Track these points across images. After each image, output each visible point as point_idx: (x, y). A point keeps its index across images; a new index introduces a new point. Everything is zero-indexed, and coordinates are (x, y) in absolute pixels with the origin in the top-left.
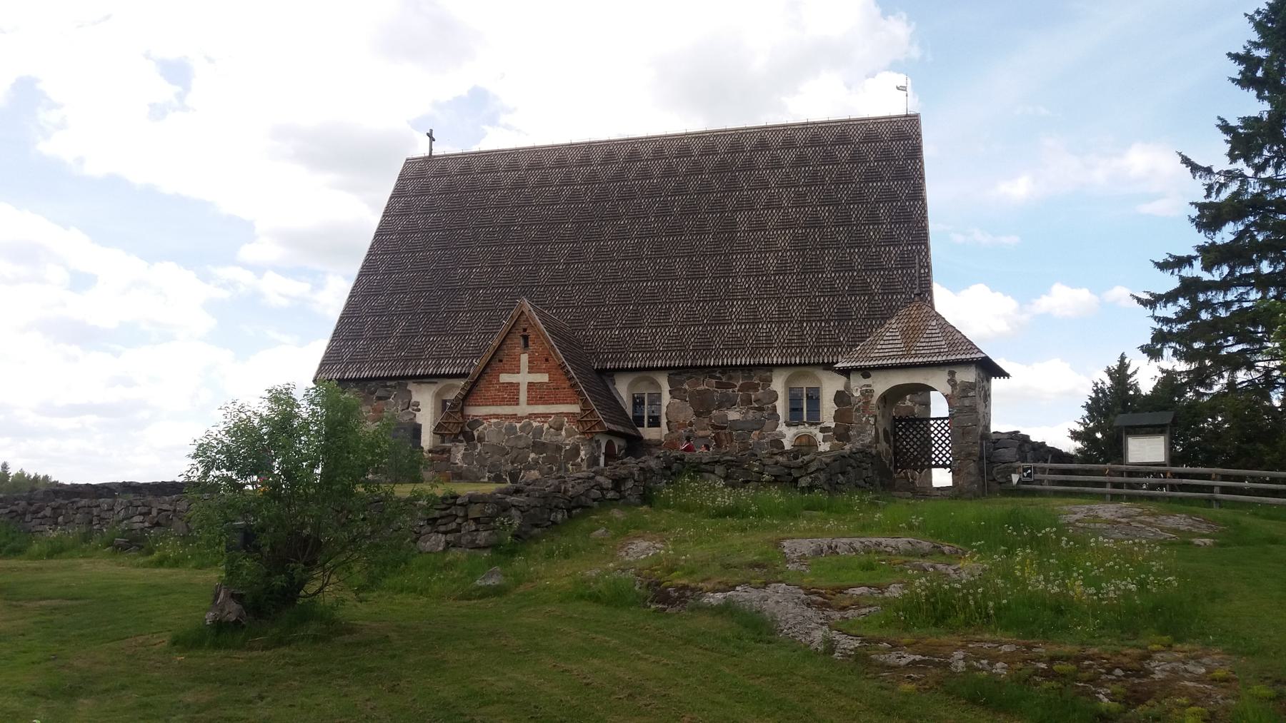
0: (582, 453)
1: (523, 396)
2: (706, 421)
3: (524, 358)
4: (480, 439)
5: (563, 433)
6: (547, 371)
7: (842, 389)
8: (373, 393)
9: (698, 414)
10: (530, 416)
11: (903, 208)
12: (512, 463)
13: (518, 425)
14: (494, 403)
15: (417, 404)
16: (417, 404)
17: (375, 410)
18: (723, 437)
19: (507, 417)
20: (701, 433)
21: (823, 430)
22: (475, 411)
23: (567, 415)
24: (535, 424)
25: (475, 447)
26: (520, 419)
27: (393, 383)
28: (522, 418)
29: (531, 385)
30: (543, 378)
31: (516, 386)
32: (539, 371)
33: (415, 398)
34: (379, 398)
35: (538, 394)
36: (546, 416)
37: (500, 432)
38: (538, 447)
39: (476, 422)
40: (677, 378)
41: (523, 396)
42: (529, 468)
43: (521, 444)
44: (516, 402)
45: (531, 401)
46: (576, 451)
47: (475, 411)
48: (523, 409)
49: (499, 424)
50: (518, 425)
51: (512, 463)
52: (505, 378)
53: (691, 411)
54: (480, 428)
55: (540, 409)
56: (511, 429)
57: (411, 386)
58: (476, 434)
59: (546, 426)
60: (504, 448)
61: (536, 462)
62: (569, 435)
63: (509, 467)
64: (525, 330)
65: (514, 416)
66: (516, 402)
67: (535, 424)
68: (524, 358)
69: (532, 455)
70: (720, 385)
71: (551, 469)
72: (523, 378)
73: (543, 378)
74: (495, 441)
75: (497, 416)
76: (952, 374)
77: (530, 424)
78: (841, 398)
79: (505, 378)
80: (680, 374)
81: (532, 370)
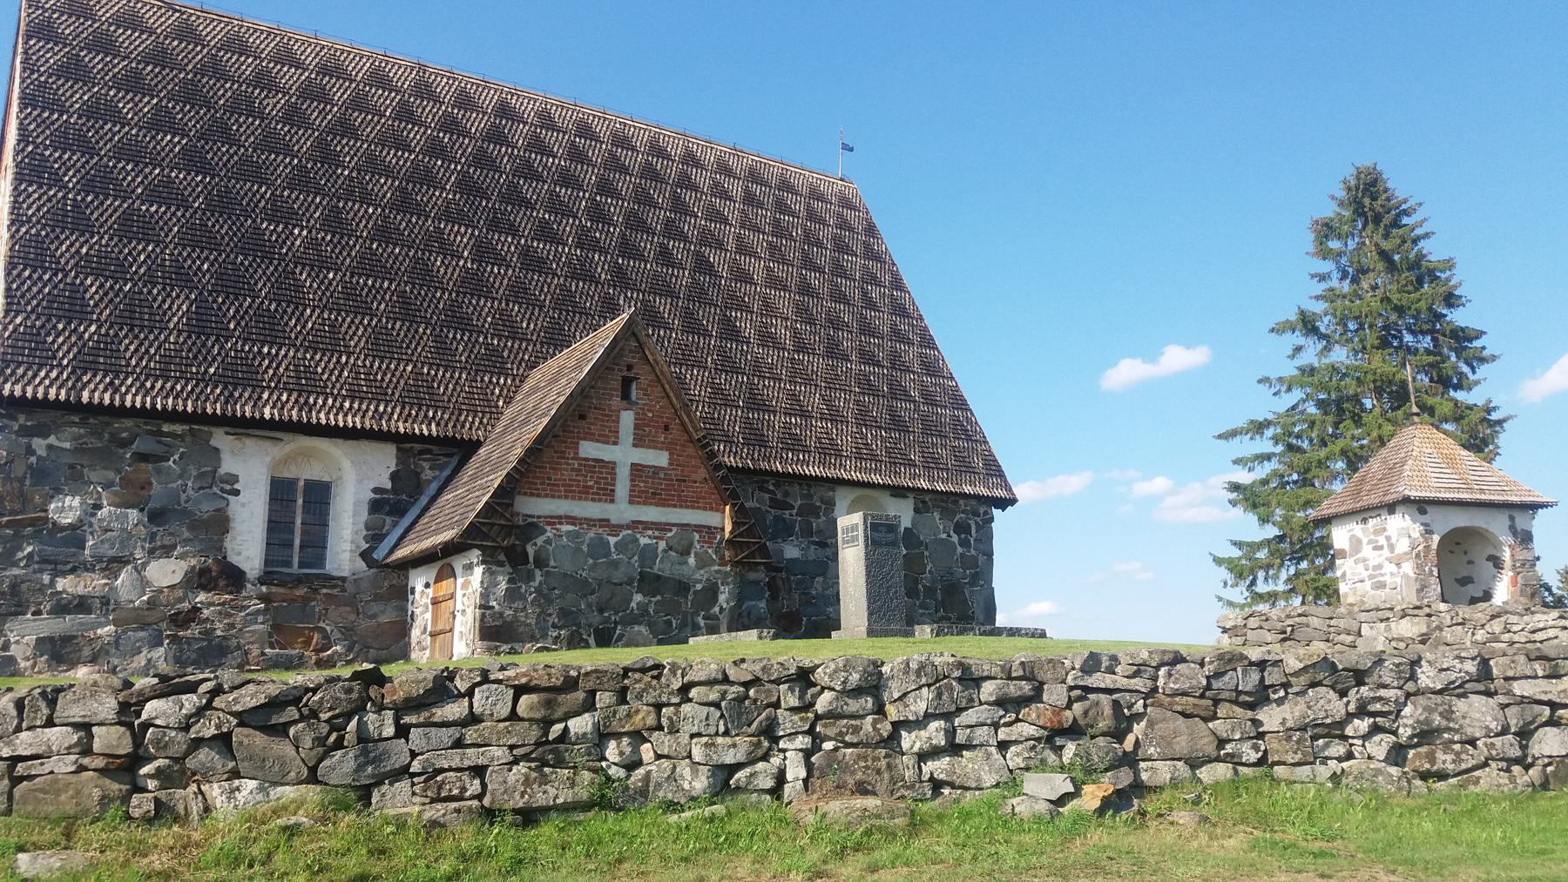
0: (722, 598)
1: (622, 487)
3: (627, 419)
4: (540, 562)
5: (692, 560)
6: (669, 447)
10: (635, 525)
12: (601, 611)
13: (612, 540)
14: (569, 494)
15: (233, 479)
16: (233, 479)
17: (126, 482)
18: (780, 583)
19: (590, 522)
22: (535, 506)
23: (699, 528)
24: (644, 541)
25: (530, 577)
26: (615, 529)
27: (179, 428)
28: (621, 527)
29: (637, 469)
30: (660, 459)
32: (654, 445)
33: (228, 465)
34: (142, 457)
35: (647, 486)
37: (578, 550)
38: (650, 582)
39: (531, 529)
41: (622, 487)
43: (618, 576)
44: (608, 495)
46: (712, 592)
47: (535, 506)
48: (622, 510)
49: (577, 535)
51: (601, 611)
52: (589, 449)
54: (540, 541)
55: (652, 513)
56: (599, 547)
57: (220, 439)
58: (531, 550)
59: (662, 545)
61: (643, 609)
62: (703, 563)
63: (596, 619)
64: (630, 368)
65: (604, 523)
66: (608, 495)
68: (627, 419)
69: (638, 598)
70: (775, 503)
71: (669, 623)
72: (624, 454)
73: (660, 459)
74: (568, 567)
75: (571, 520)
79: (589, 449)
81: (639, 442)
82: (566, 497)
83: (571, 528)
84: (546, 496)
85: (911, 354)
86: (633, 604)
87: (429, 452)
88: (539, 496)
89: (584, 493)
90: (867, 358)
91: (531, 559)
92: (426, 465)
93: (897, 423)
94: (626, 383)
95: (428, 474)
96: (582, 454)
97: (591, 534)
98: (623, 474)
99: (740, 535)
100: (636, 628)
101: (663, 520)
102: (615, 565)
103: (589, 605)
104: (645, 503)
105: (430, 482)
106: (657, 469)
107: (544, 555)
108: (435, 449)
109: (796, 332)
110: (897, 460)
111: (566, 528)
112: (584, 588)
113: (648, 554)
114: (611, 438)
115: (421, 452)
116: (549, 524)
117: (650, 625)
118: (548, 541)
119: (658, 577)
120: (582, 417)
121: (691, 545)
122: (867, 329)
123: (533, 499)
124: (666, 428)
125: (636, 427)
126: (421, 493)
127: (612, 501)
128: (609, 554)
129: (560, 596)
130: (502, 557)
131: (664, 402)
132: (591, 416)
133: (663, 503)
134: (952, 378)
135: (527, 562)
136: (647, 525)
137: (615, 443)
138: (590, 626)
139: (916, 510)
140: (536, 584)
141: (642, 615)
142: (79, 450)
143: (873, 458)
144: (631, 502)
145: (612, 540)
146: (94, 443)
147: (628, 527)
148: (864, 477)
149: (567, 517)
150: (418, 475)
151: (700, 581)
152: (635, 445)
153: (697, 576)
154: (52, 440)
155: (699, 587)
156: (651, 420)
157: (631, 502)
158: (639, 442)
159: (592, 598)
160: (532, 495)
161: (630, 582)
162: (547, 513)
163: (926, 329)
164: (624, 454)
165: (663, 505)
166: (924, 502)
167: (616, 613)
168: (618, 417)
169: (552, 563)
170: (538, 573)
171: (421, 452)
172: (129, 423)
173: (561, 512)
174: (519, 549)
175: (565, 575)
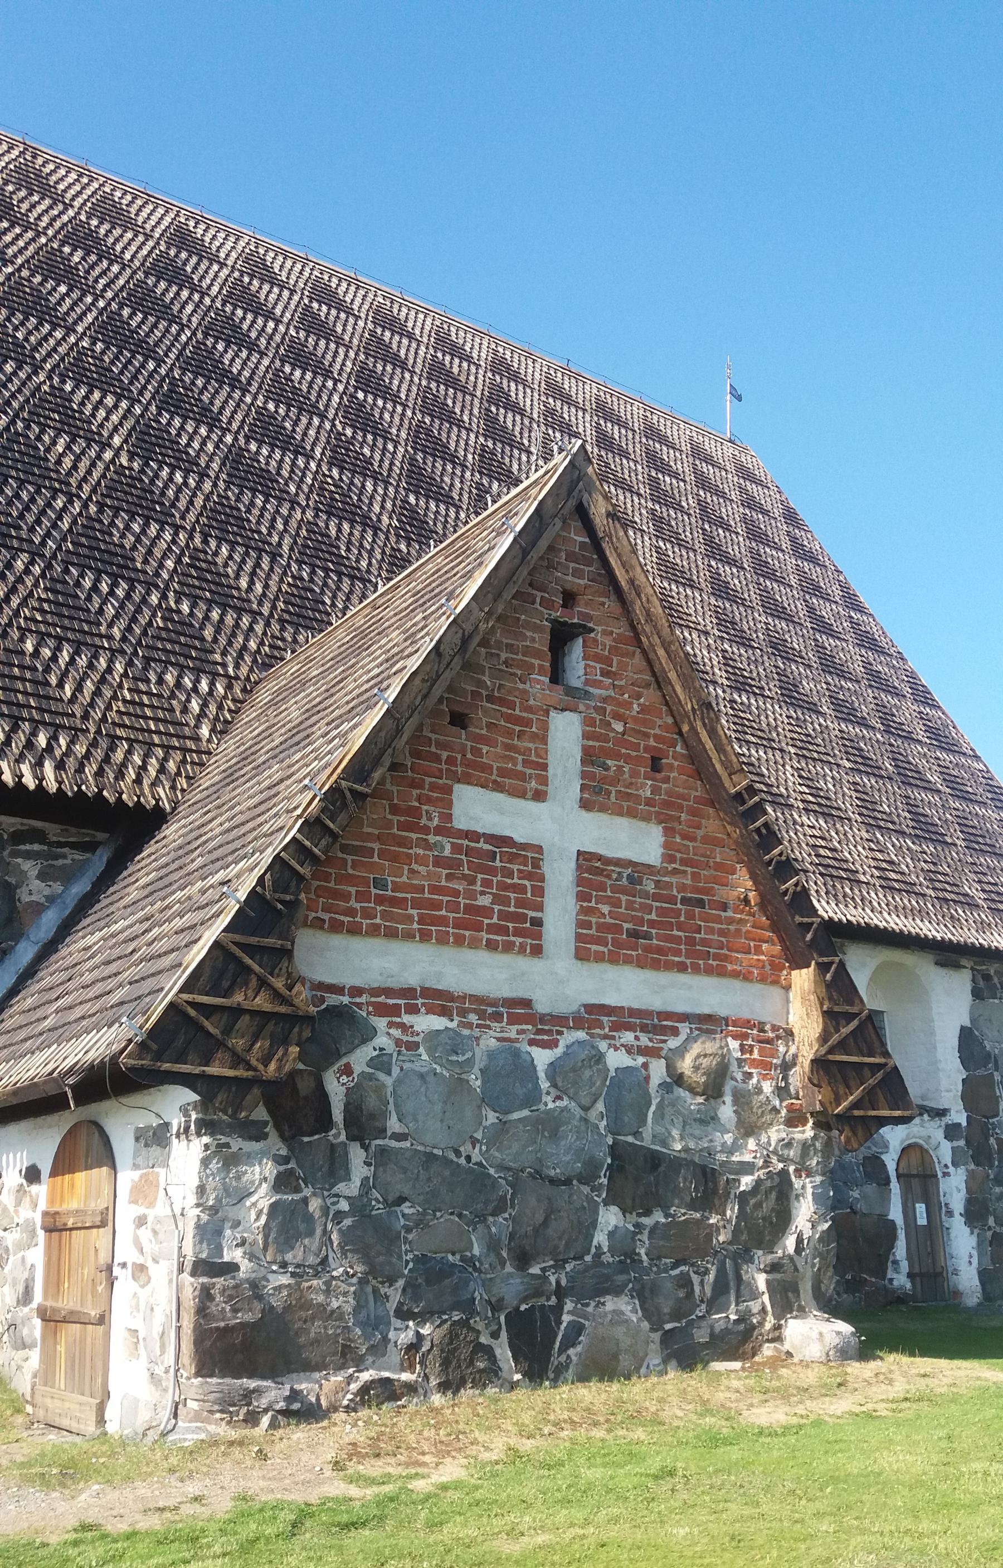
1: (560, 915)
3: (565, 734)
4: (363, 1124)
6: (663, 813)
7: (967, 1023)
10: (593, 1015)
12: (523, 1260)
13: (542, 1058)
14: (430, 930)
19: (489, 1009)
21: (952, 1132)
22: (343, 961)
24: (616, 1060)
25: (336, 1167)
26: (547, 1026)
28: (560, 1021)
29: (591, 866)
30: (639, 842)
31: (527, 857)
32: (629, 807)
35: (626, 917)
39: (330, 1026)
41: (560, 915)
42: (600, 1284)
43: (561, 1157)
44: (523, 933)
45: (593, 944)
46: (780, 1191)
47: (343, 961)
48: (560, 978)
51: (523, 1260)
52: (477, 809)
54: (360, 1059)
55: (628, 986)
58: (336, 1088)
60: (479, 1179)
63: (511, 1285)
65: (519, 1010)
66: (523, 933)
68: (565, 734)
69: (610, 1218)
73: (639, 842)
74: (435, 1137)
75: (440, 1000)
77: (599, 1058)
78: (969, 1042)
79: (477, 809)
81: (595, 796)
82: (425, 937)
83: (437, 1023)
84: (374, 931)
85: (907, 712)
86: (601, 1238)
87: (39, 836)
88: (354, 930)
89: (467, 928)
90: (845, 712)
91: (338, 1114)
92: (30, 868)
93: (925, 830)
94: (561, 637)
95: (34, 889)
96: (461, 822)
97: (489, 1041)
98: (560, 878)
99: (842, 1046)
100: (611, 1304)
101: (656, 1003)
102: (551, 1125)
103: (493, 1245)
104: (613, 959)
105: (38, 909)
106: (639, 870)
107: (371, 1102)
108: (53, 830)
109: (727, 660)
110: (951, 899)
111: (427, 1023)
112: (476, 1192)
113: (627, 1095)
114: (528, 782)
115: (19, 837)
116: (383, 1010)
117: (645, 1295)
118: (381, 1062)
119: (654, 1160)
120: (459, 720)
122: (830, 665)
123: (338, 941)
124: (656, 765)
125: (589, 757)
126: (18, 936)
127: (537, 951)
128: (532, 1098)
129: (420, 1223)
130: (261, 1113)
131: (650, 696)
132: (481, 718)
133: (654, 960)
134: (977, 757)
135: (325, 1122)
136: (624, 1019)
137: (539, 796)
138: (496, 1307)
139: (977, 994)
140: (352, 1188)
141: (622, 1267)
143: (909, 889)
144: (581, 955)
145: (542, 1058)
147: (578, 1023)
148: (895, 922)
149: (427, 992)
150: (10, 891)
151: (747, 1168)
152: (585, 805)
155: (746, 1182)
156: (621, 740)
157: (581, 955)
158: (595, 796)
159: (499, 1224)
160: (336, 927)
161: (587, 1178)
162: (374, 980)
163: (913, 676)
164: (560, 826)
165: (656, 965)
166: (987, 978)
167: (559, 1265)
168: (545, 727)
169: (393, 1124)
170: (357, 1155)
171: (19, 837)
173: (412, 980)
174: (305, 1086)
175: (430, 1157)
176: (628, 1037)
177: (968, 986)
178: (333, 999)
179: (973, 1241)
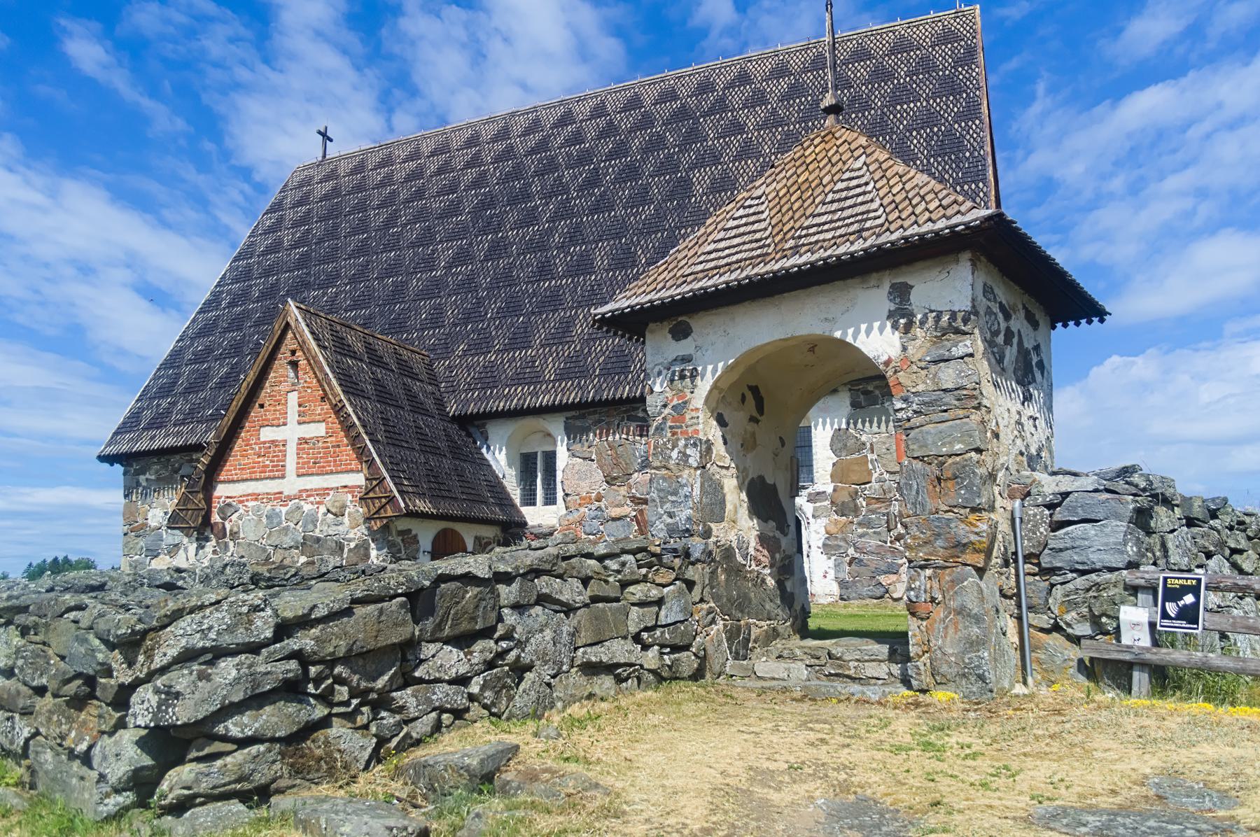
2: (623, 491)
4: (234, 535)
5: (346, 520)
8: (176, 472)
9: (610, 481)
10: (303, 494)
11: (949, 133)
13: (284, 510)
20: (616, 512)
24: (307, 507)
28: (290, 498)
29: (303, 441)
30: (319, 430)
36: (324, 492)
40: (578, 423)
43: (287, 541)
48: (291, 484)
50: (284, 510)
52: (267, 434)
53: (599, 476)
54: (234, 517)
59: (323, 509)
64: (293, 352)
65: (279, 496)
67: (307, 507)
72: (291, 433)
73: (319, 430)
74: (252, 537)
75: (256, 496)
76: (901, 292)
77: (299, 508)
79: (267, 434)
80: (583, 417)
98: (291, 450)
111: (250, 504)
119: (318, 540)
121: (344, 507)
127: (283, 477)
139: (855, 405)
142: (158, 479)
146: (165, 473)
151: (350, 540)
152: (299, 423)
153: (351, 535)
154: (148, 476)
155: (352, 545)
170: (231, 544)
172: (178, 457)
176: (312, 499)
177: (848, 403)
178: (228, 501)
179: (831, 563)
